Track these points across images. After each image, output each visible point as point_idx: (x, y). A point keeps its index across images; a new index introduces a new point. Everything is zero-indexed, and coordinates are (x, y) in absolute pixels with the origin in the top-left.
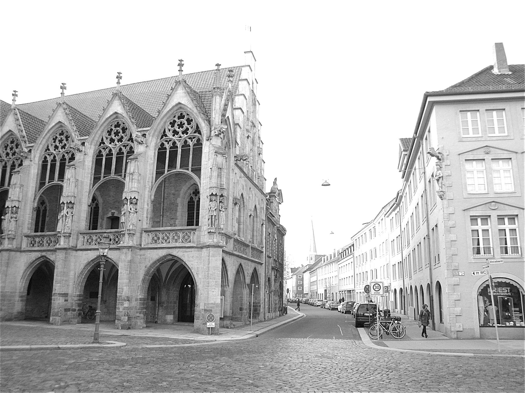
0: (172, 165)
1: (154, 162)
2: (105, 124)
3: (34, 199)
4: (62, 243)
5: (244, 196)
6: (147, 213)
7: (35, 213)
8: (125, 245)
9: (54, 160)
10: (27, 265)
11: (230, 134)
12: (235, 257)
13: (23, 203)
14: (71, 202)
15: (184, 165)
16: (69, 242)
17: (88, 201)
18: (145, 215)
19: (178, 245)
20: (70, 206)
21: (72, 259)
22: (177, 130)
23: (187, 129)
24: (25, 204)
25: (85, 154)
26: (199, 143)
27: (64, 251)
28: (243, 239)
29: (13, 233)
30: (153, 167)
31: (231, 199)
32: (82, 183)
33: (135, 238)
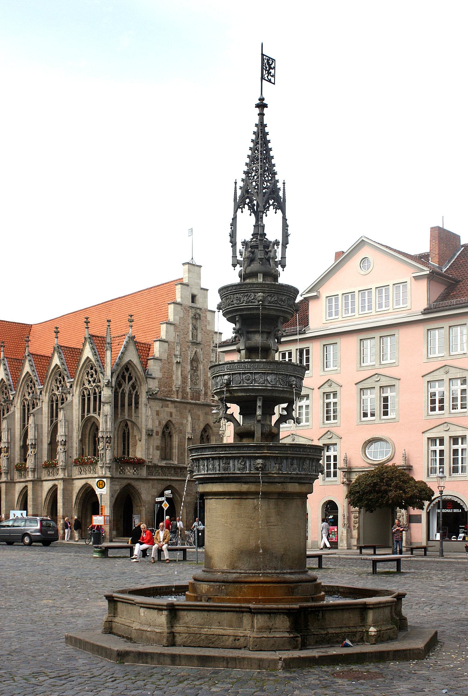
0: (89, 411)
1: (79, 408)
2: (53, 374)
3: (20, 439)
4: (30, 476)
5: (174, 422)
6: (76, 451)
7: (23, 450)
8: (59, 477)
9: (28, 405)
10: (19, 493)
11: (139, 374)
12: (156, 482)
13: (12, 444)
14: (32, 444)
15: (95, 410)
16: (34, 475)
17: (48, 440)
18: (74, 452)
19: (90, 475)
20: (33, 446)
21: (39, 488)
22: (90, 380)
23: (95, 379)
24: (14, 444)
25: (42, 402)
26: (100, 393)
27: (31, 483)
28: (176, 463)
29: (6, 468)
30: (79, 412)
31: (144, 431)
32: (42, 425)
33: (66, 471)
